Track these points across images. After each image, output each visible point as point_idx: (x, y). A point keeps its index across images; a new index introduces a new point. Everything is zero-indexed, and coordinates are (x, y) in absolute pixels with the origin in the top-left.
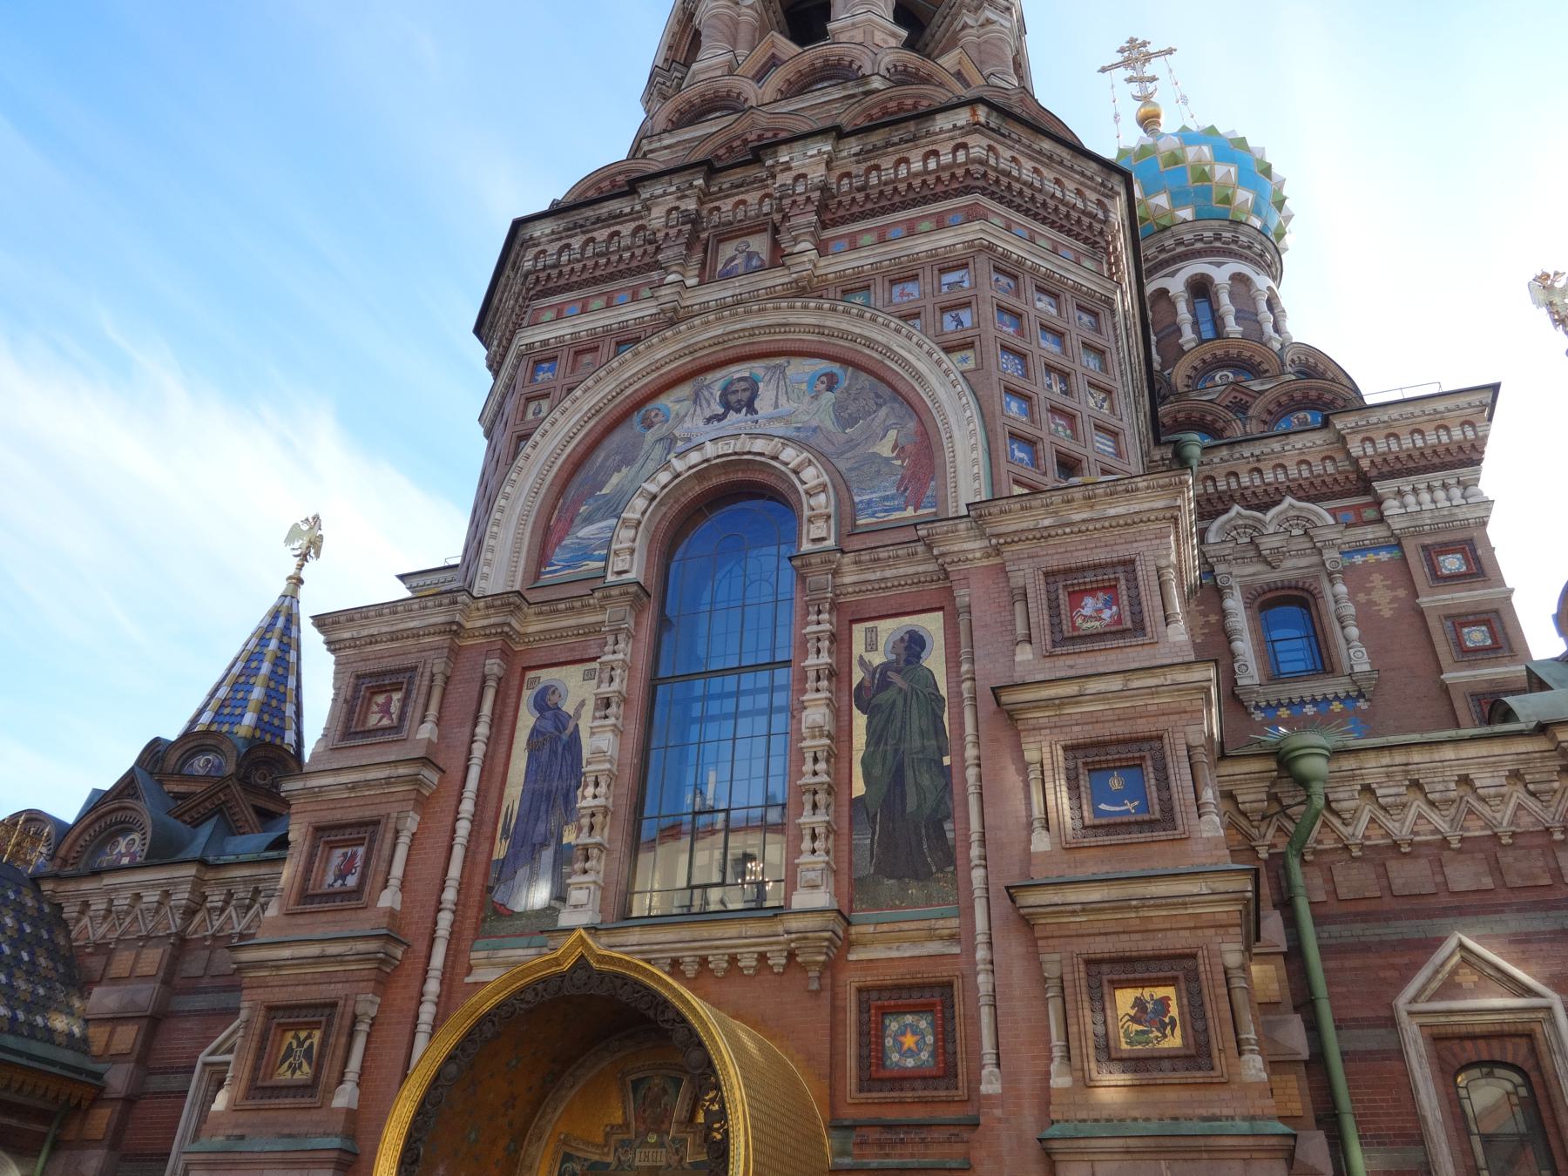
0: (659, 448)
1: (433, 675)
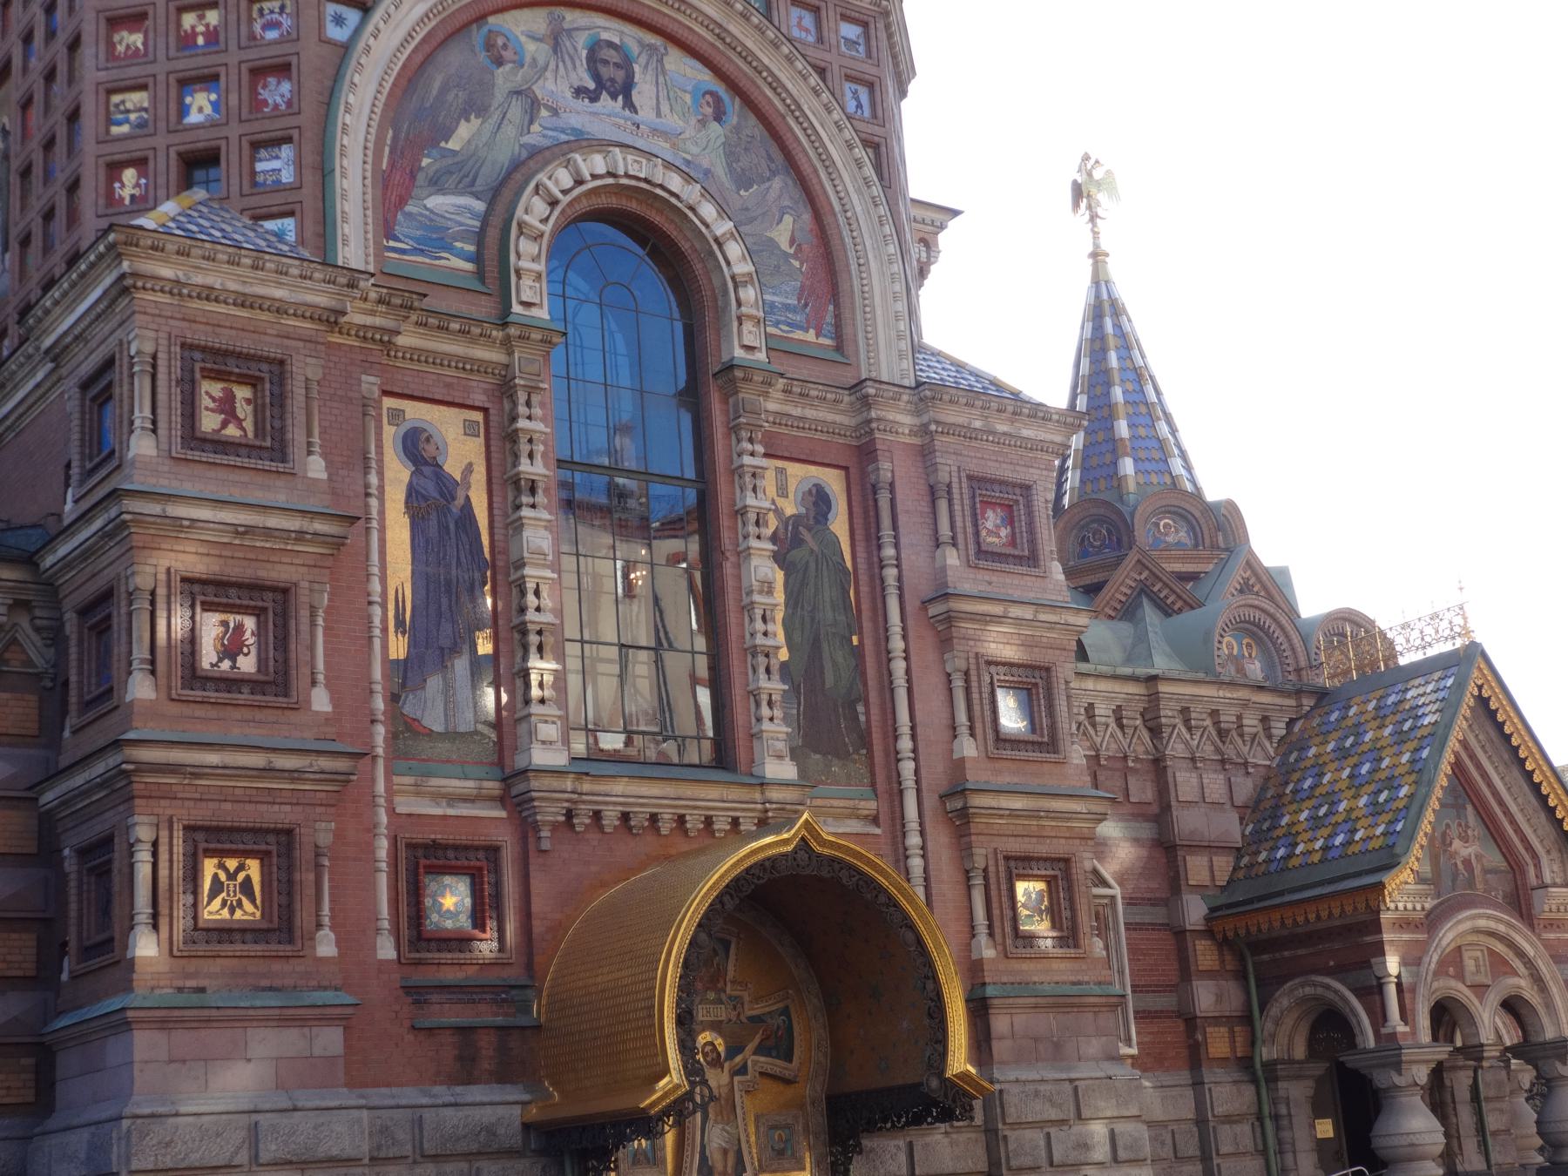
0: (516, 110)
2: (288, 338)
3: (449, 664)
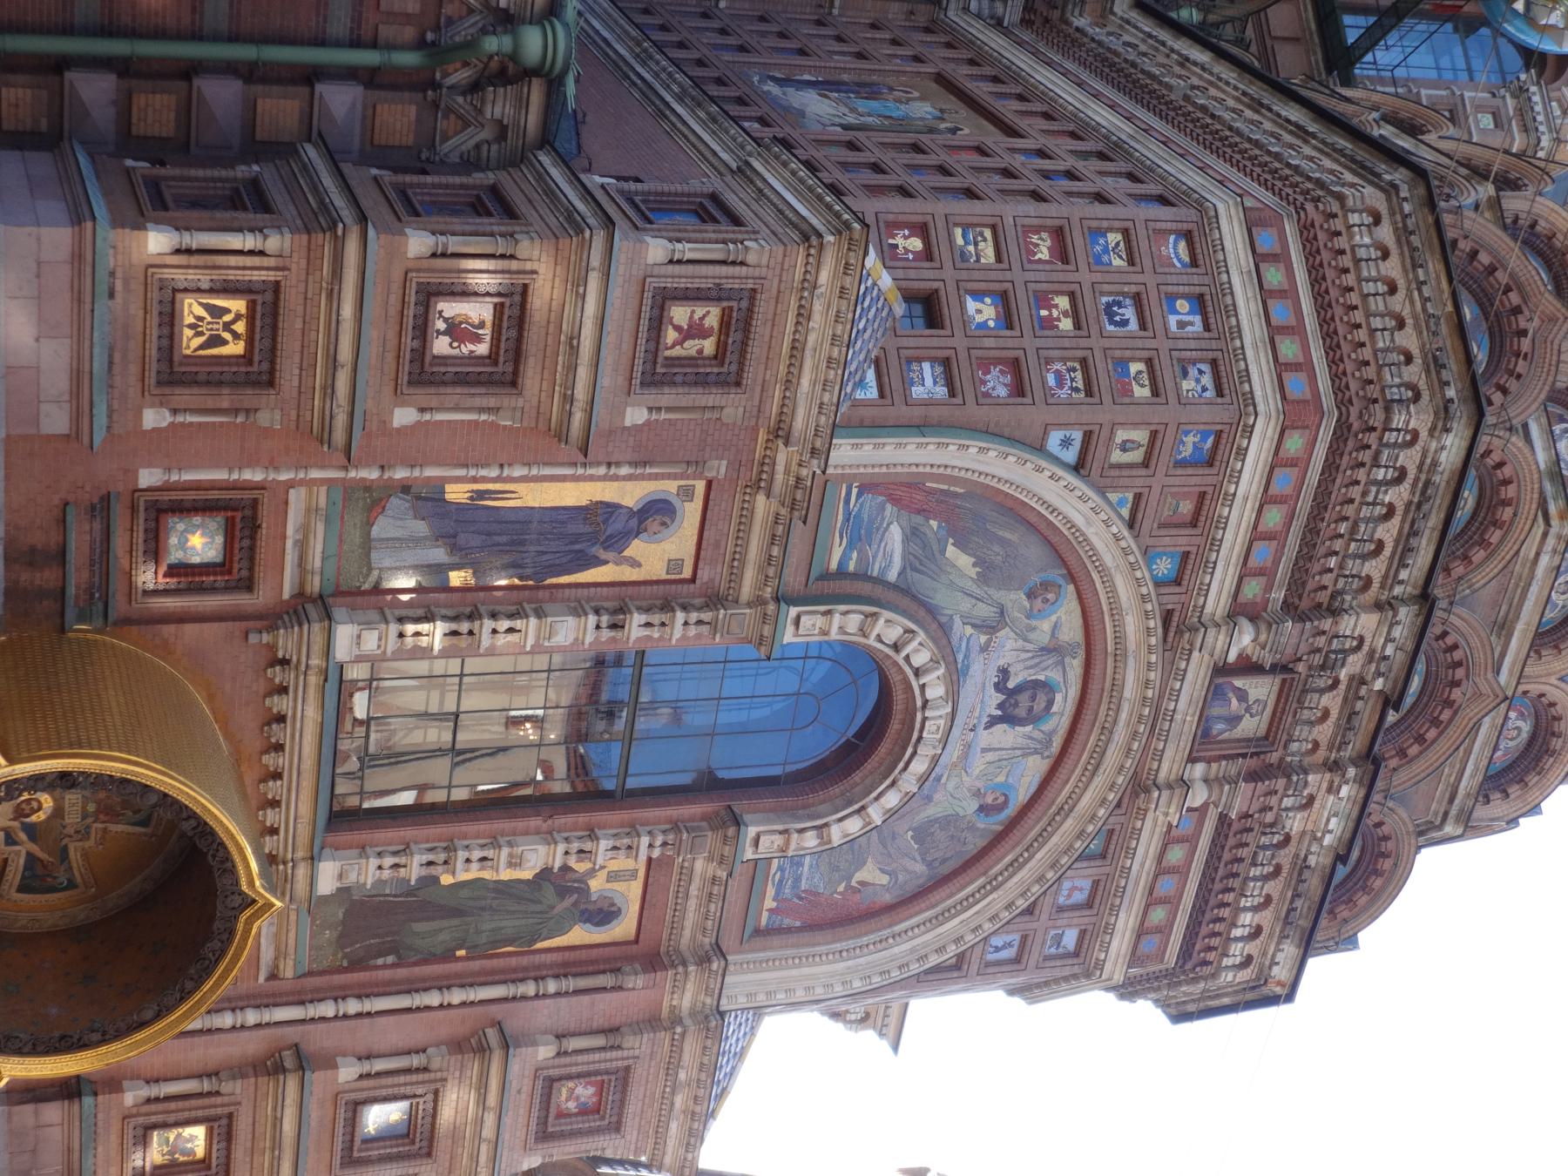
0: (985, 611)
3: (439, 543)
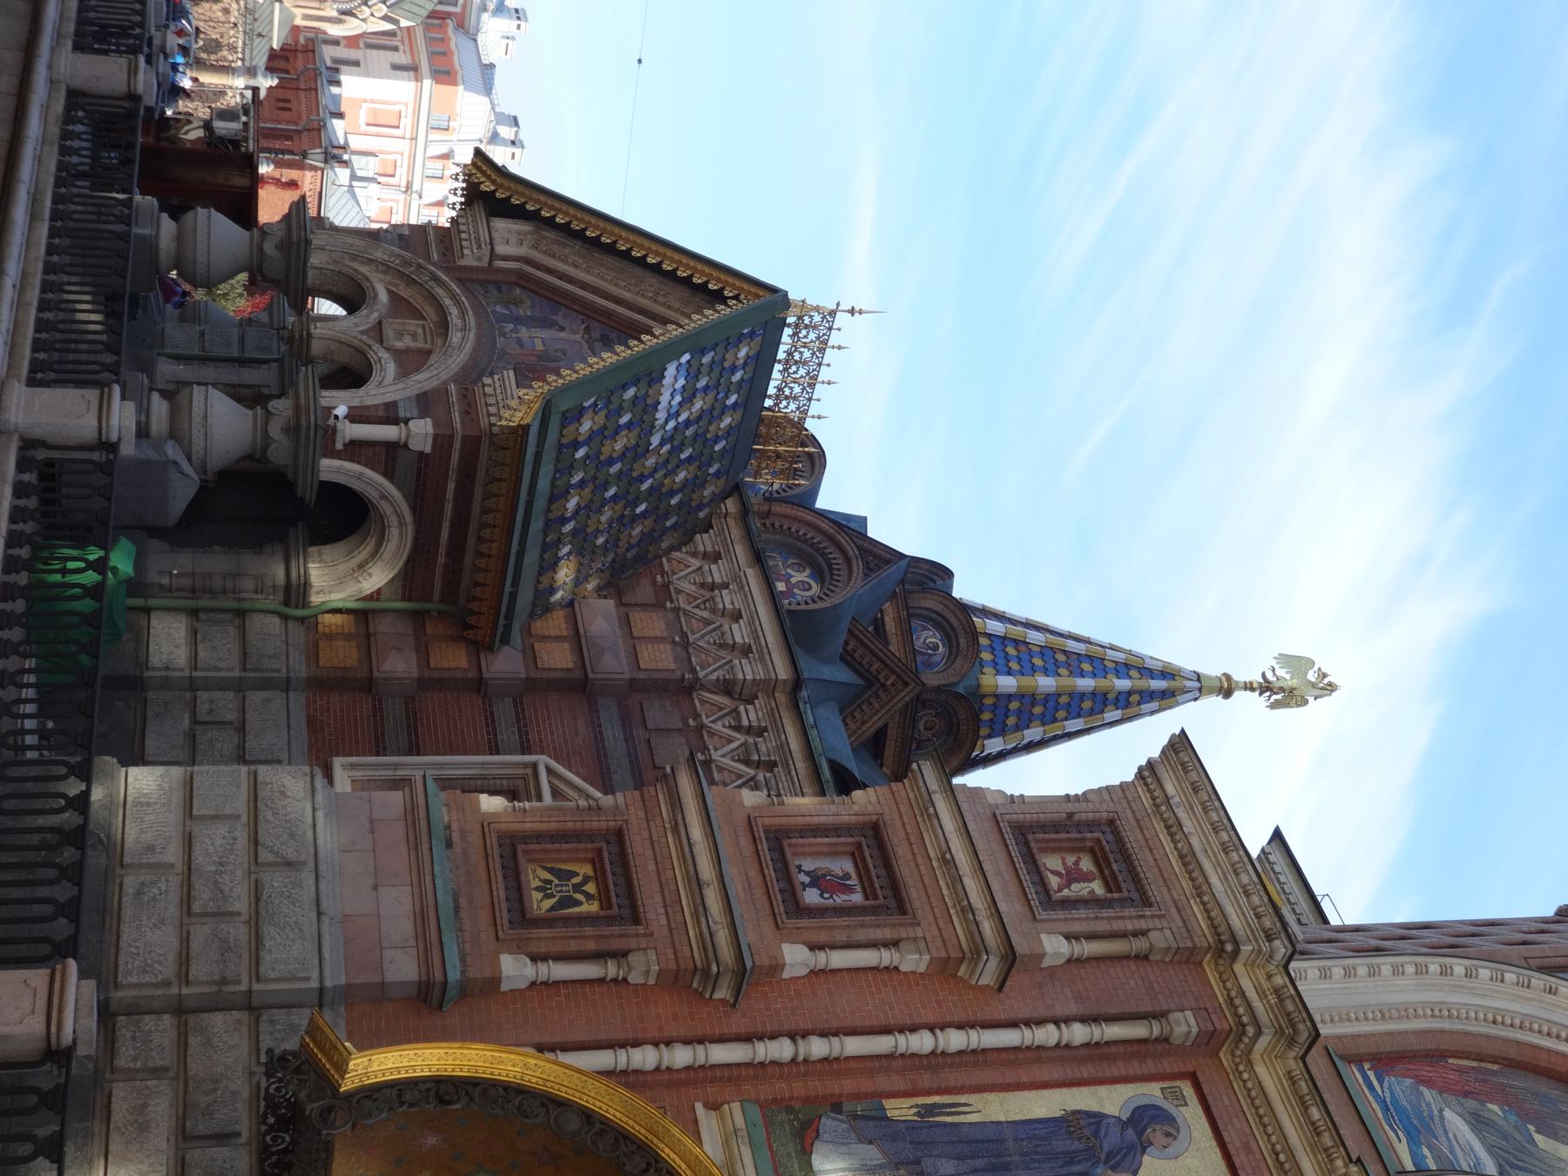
1: (1144, 933)
2: (1179, 911)
